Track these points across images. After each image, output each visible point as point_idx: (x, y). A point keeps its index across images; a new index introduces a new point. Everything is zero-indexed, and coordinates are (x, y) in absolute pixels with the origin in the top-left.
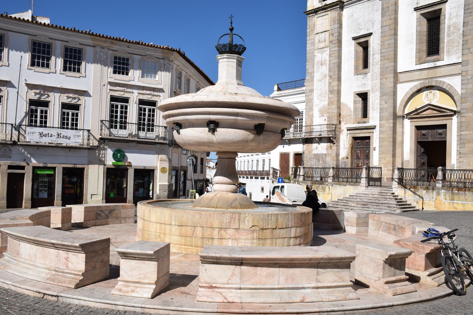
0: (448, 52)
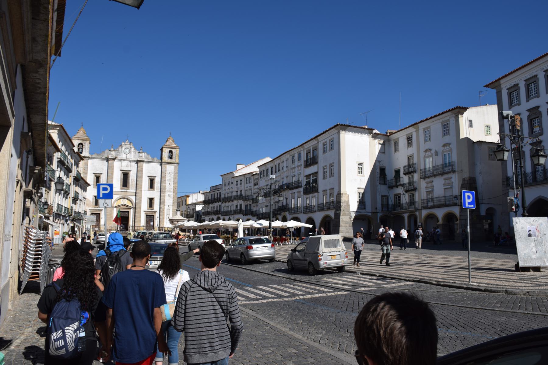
0: (131, 188)
